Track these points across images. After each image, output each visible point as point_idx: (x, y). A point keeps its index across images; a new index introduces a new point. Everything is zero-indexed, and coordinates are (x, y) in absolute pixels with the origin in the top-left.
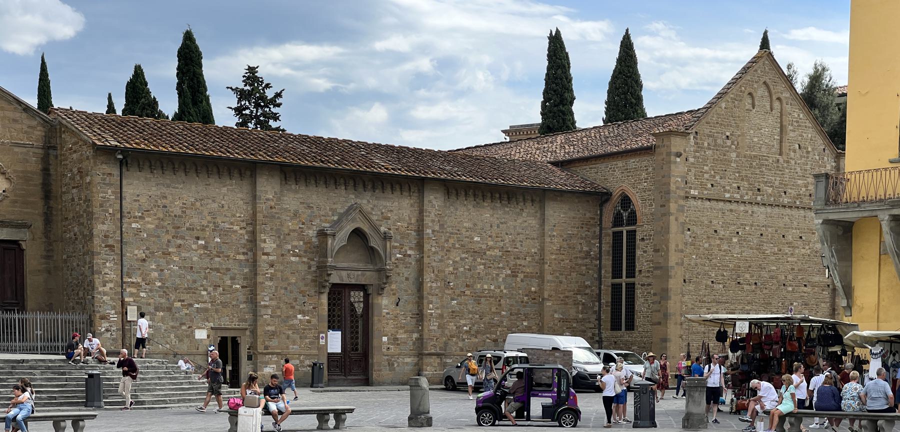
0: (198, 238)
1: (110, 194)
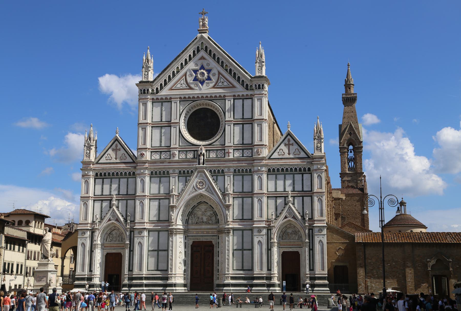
0: (388, 264)
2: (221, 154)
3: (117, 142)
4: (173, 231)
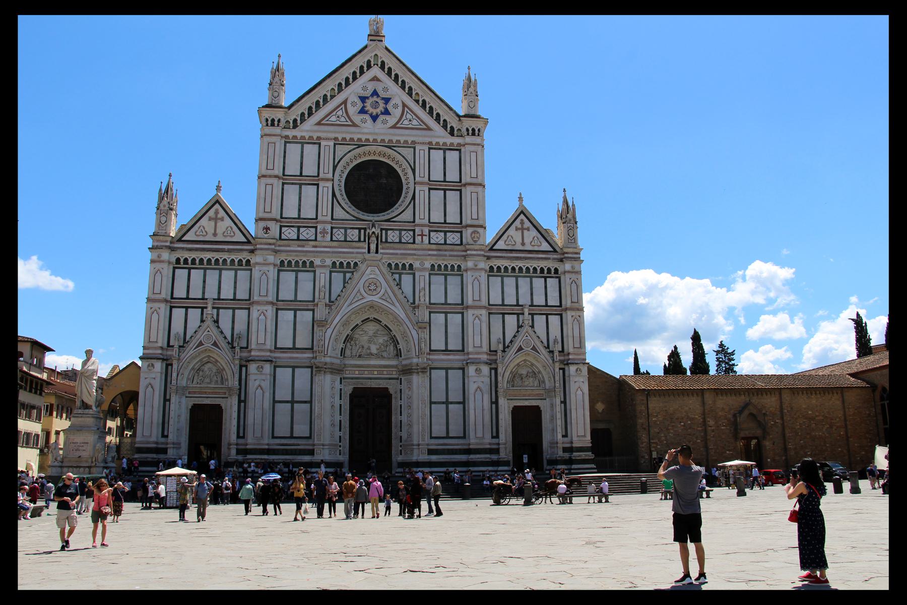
0: (681, 422)
1: (643, 408)
2: (407, 237)
3: (217, 206)
4: (322, 367)
